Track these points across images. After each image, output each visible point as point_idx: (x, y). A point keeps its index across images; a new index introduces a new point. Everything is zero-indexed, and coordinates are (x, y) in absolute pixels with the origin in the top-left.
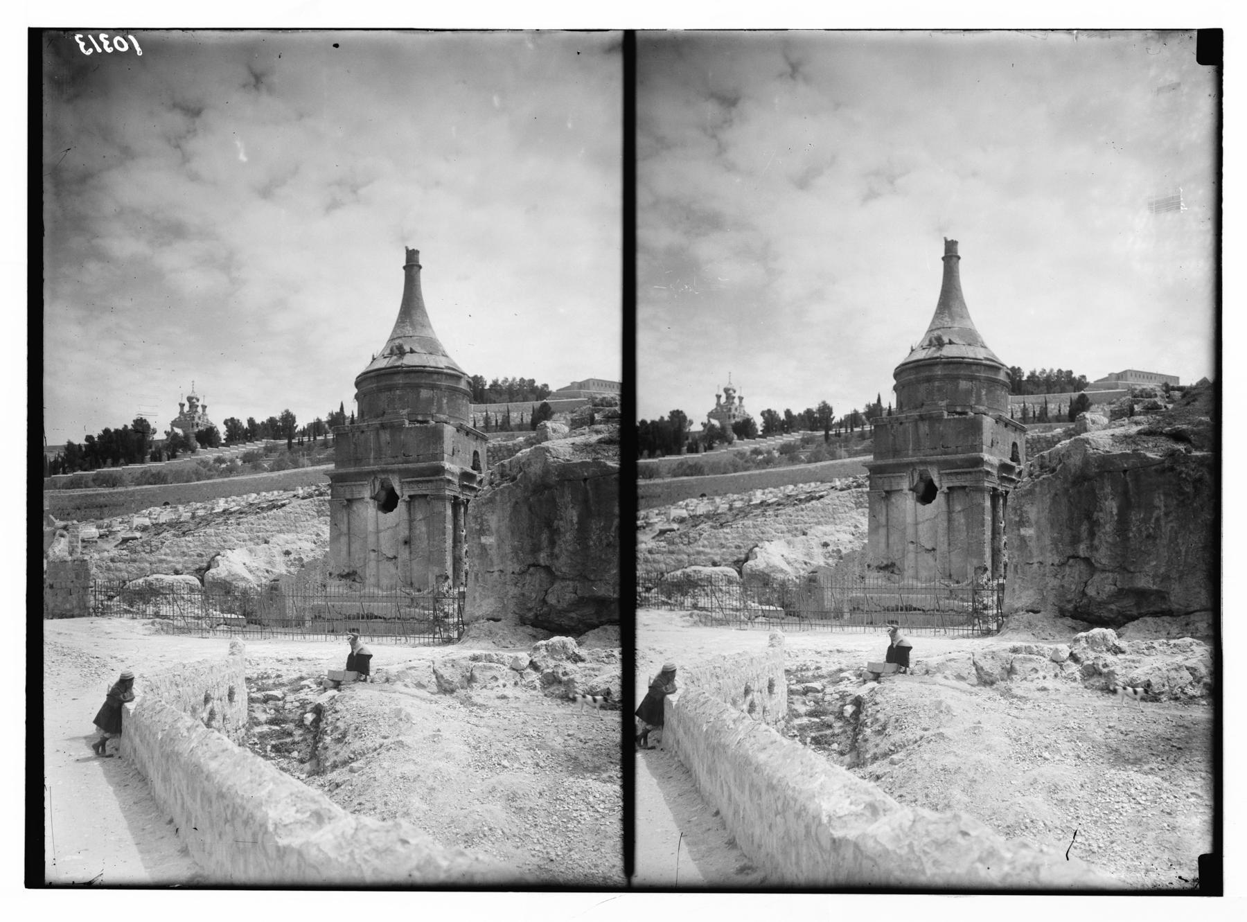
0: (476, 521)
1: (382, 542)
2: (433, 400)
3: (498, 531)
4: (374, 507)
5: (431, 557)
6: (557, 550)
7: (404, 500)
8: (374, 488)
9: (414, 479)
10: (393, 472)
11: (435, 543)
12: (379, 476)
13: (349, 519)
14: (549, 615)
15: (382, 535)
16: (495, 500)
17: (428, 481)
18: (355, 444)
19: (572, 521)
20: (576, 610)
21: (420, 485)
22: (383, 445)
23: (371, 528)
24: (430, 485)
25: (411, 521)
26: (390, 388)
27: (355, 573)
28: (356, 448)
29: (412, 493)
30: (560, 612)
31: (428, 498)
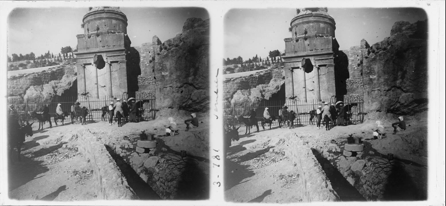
0: (368, 69)
2: (325, 28)
3: (378, 72)
5: (329, 89)
6: (404, 80)
9: (320, 59)
11: (330, 84)
14: (399, 108)
16: (376, 59)
17: (326, 59)
18: (294, 45)
19: (412, 66)
20: (411, 105)
22: (306, 45)
26: (308, 22)
28: (294, 47)
30: (405, 106)
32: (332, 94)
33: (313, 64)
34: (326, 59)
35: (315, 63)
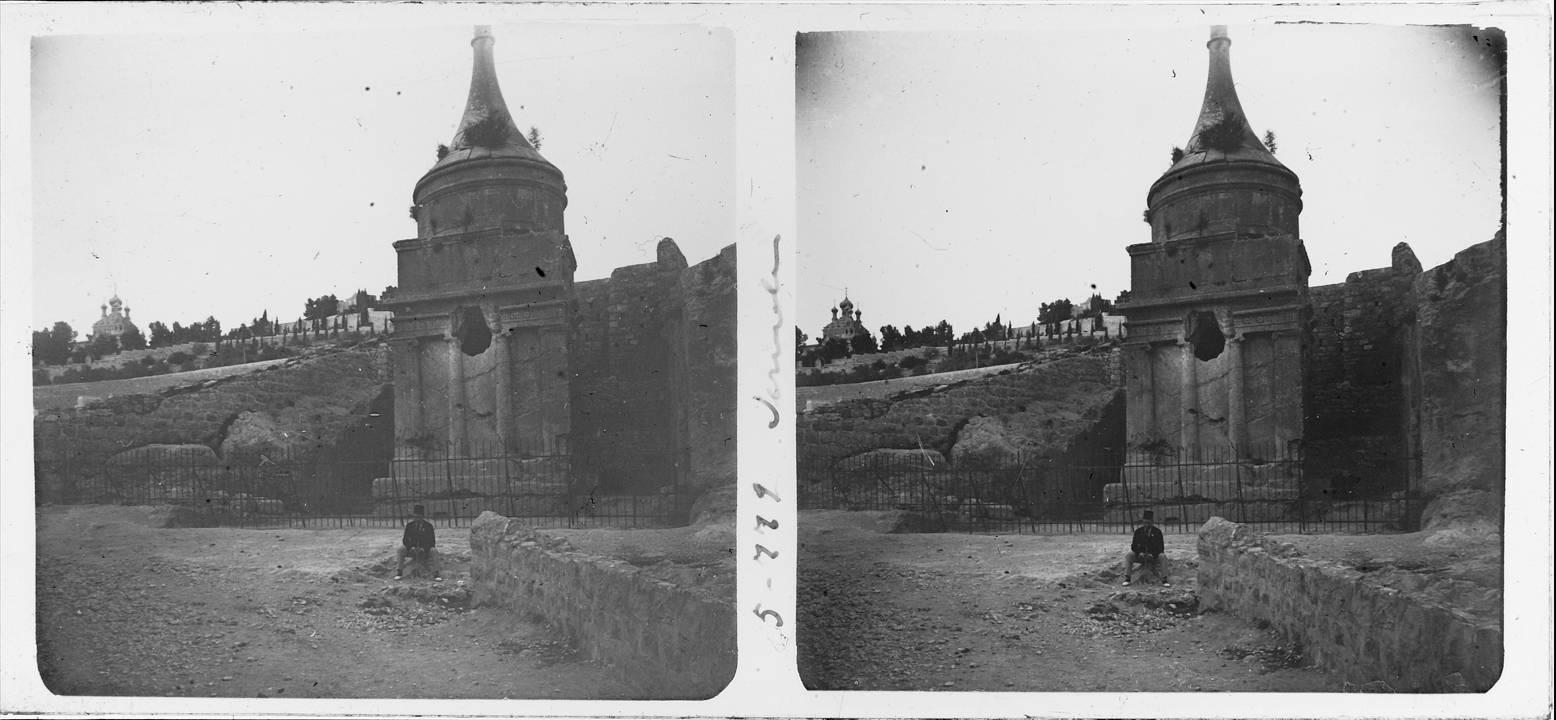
1: (1203, 399)
4: (1191, 352)
7: (1237, 341)
8: (1190, 326)
10: (1220, 302)
12: (1199, 310)
13: (1152, 369)
15: (1202, 389)
17: (1272, 313)
21: (1260, 319)
23: (1186, 379)
24: (1275, 319)
25: (1245, 366)
27: (1163, 442)
29: (1248, 330)
31: (1273, 336)
32: (1289, 434)
33: (1225, 331)
34: (1272, 313)
35: (1231, 325)
